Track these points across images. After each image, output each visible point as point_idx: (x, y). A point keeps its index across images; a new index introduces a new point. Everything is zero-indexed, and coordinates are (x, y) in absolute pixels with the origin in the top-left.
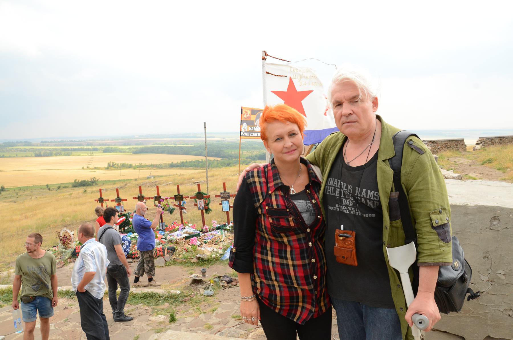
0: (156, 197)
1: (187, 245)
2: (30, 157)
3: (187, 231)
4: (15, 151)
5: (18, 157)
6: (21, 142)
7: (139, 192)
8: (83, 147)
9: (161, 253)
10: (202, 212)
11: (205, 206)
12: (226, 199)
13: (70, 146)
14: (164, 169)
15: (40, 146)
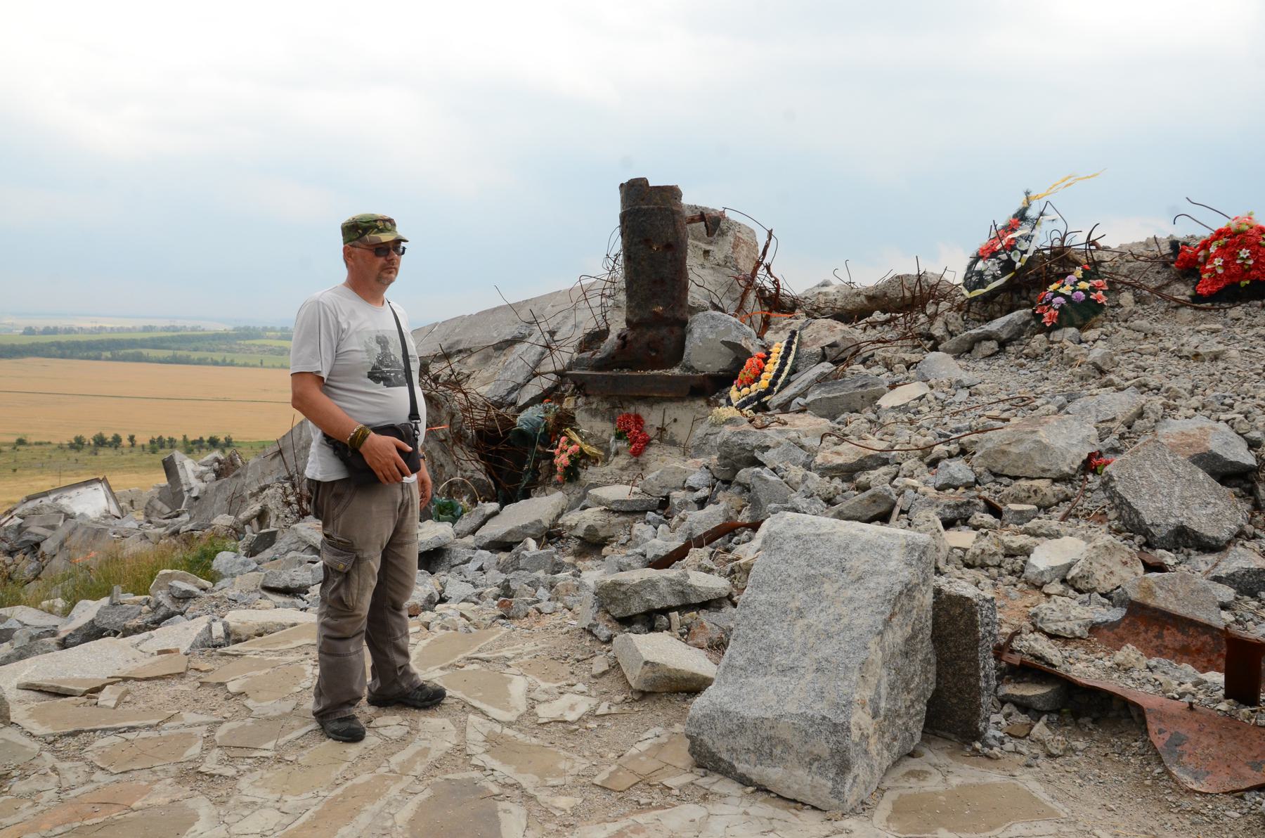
5: (265, 367)
6: (273, 329)
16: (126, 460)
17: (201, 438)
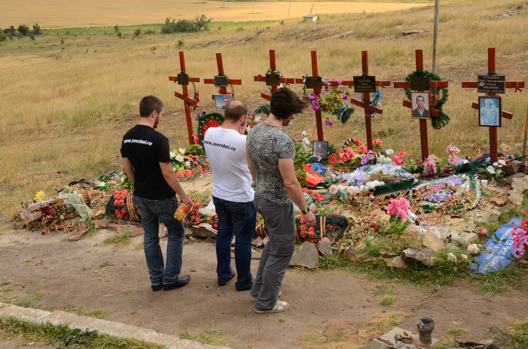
0: (308, 79)
1: (378, 211)
3: (381, 172)
7: (269, 67)
9: (311, 232)
10: (423, 123)
11: (431, 107)
12: (491, 94)
17: (12, 27)
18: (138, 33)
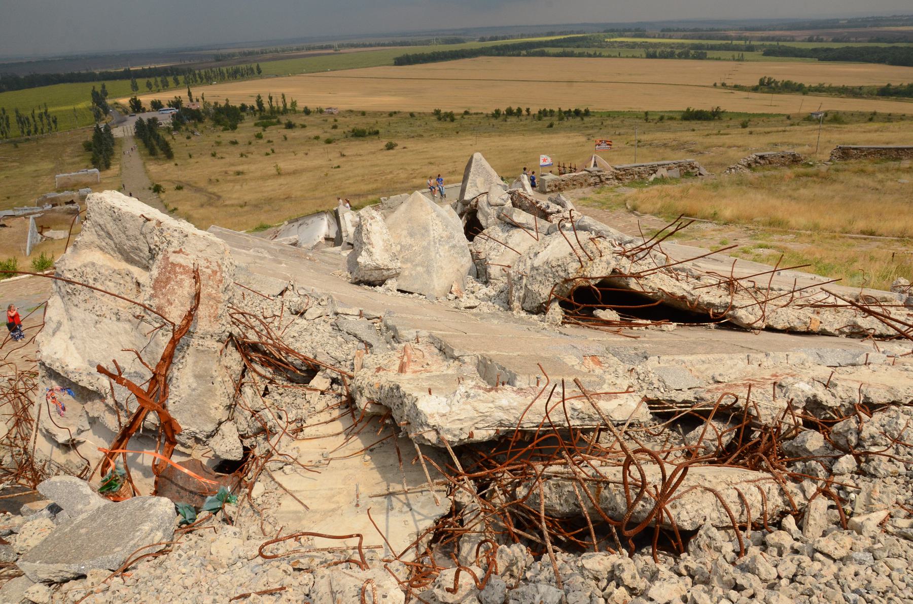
2: (638, 57)
4: (618, 47)
6: (629, 30)
8: (730, 42)
13: (707, 39)
14: (865, 98)
15: (659, 38)
16: (522, 125)
18: (662, 119)
